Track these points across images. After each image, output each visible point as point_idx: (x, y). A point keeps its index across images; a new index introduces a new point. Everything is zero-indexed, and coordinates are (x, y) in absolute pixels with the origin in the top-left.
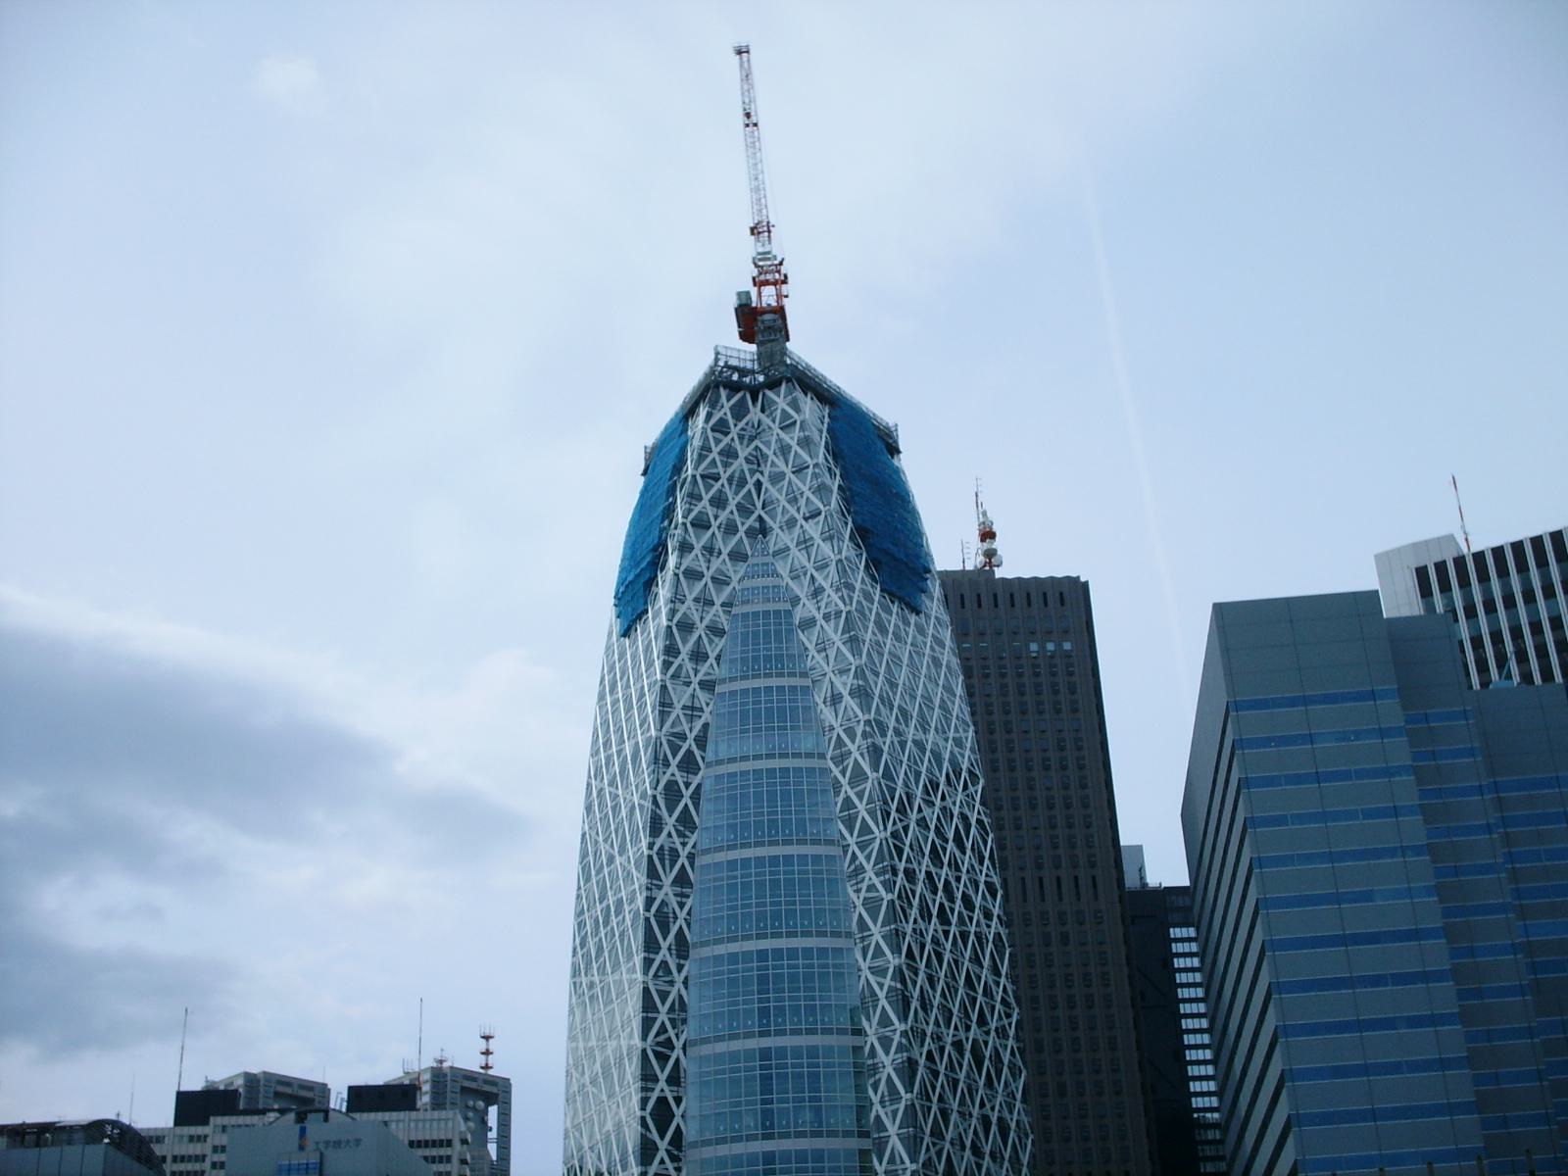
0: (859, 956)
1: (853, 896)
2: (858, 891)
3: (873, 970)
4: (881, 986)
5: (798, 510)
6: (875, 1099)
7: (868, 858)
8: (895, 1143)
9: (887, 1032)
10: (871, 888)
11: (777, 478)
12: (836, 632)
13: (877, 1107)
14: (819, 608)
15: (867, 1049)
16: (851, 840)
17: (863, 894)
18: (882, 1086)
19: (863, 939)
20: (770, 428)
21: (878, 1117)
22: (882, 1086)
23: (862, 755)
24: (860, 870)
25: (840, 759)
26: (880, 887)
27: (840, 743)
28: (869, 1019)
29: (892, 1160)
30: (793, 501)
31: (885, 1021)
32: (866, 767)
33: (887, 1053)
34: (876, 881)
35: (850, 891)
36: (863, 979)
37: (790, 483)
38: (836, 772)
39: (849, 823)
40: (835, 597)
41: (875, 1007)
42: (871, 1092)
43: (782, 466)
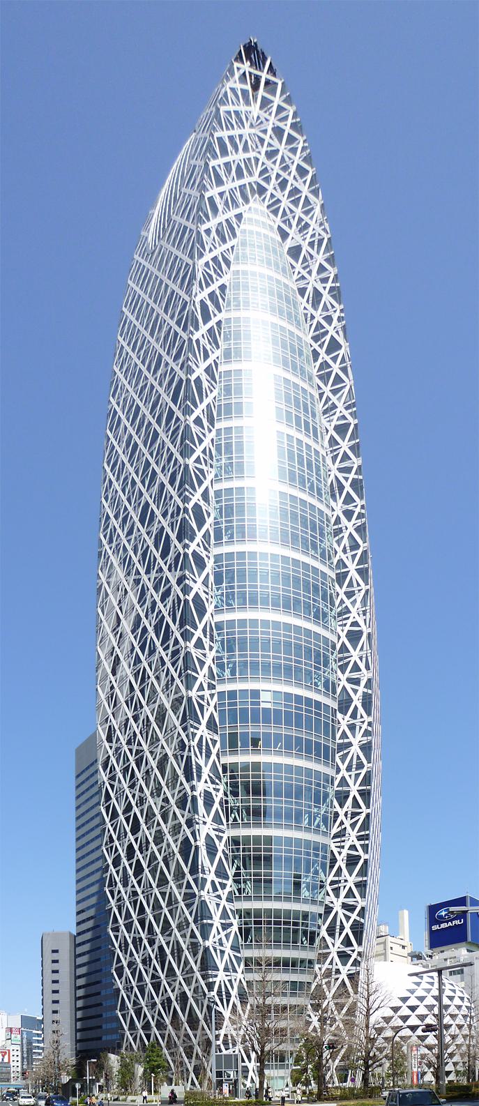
0: (329, 461)
1: (327, 425)
3: (340, 470)
4: (347, 479)
7: (339, 399)
8: (353, 574)
9: (350, 507)
12: (318, 252)
13: (340, 554)
17: (333, 424)
20: (267, 120)
21: (341, 561)
22: (345, 541)
23: (337, 332)
26: (348, 416)
28: (335, 500)
29: (350, 584)
30: (285, 168)
32: (341, 340)
33: (349, 520)
34: (346, 413)
37: (283, 157)
38: (316, 346)
42: (335, 545)
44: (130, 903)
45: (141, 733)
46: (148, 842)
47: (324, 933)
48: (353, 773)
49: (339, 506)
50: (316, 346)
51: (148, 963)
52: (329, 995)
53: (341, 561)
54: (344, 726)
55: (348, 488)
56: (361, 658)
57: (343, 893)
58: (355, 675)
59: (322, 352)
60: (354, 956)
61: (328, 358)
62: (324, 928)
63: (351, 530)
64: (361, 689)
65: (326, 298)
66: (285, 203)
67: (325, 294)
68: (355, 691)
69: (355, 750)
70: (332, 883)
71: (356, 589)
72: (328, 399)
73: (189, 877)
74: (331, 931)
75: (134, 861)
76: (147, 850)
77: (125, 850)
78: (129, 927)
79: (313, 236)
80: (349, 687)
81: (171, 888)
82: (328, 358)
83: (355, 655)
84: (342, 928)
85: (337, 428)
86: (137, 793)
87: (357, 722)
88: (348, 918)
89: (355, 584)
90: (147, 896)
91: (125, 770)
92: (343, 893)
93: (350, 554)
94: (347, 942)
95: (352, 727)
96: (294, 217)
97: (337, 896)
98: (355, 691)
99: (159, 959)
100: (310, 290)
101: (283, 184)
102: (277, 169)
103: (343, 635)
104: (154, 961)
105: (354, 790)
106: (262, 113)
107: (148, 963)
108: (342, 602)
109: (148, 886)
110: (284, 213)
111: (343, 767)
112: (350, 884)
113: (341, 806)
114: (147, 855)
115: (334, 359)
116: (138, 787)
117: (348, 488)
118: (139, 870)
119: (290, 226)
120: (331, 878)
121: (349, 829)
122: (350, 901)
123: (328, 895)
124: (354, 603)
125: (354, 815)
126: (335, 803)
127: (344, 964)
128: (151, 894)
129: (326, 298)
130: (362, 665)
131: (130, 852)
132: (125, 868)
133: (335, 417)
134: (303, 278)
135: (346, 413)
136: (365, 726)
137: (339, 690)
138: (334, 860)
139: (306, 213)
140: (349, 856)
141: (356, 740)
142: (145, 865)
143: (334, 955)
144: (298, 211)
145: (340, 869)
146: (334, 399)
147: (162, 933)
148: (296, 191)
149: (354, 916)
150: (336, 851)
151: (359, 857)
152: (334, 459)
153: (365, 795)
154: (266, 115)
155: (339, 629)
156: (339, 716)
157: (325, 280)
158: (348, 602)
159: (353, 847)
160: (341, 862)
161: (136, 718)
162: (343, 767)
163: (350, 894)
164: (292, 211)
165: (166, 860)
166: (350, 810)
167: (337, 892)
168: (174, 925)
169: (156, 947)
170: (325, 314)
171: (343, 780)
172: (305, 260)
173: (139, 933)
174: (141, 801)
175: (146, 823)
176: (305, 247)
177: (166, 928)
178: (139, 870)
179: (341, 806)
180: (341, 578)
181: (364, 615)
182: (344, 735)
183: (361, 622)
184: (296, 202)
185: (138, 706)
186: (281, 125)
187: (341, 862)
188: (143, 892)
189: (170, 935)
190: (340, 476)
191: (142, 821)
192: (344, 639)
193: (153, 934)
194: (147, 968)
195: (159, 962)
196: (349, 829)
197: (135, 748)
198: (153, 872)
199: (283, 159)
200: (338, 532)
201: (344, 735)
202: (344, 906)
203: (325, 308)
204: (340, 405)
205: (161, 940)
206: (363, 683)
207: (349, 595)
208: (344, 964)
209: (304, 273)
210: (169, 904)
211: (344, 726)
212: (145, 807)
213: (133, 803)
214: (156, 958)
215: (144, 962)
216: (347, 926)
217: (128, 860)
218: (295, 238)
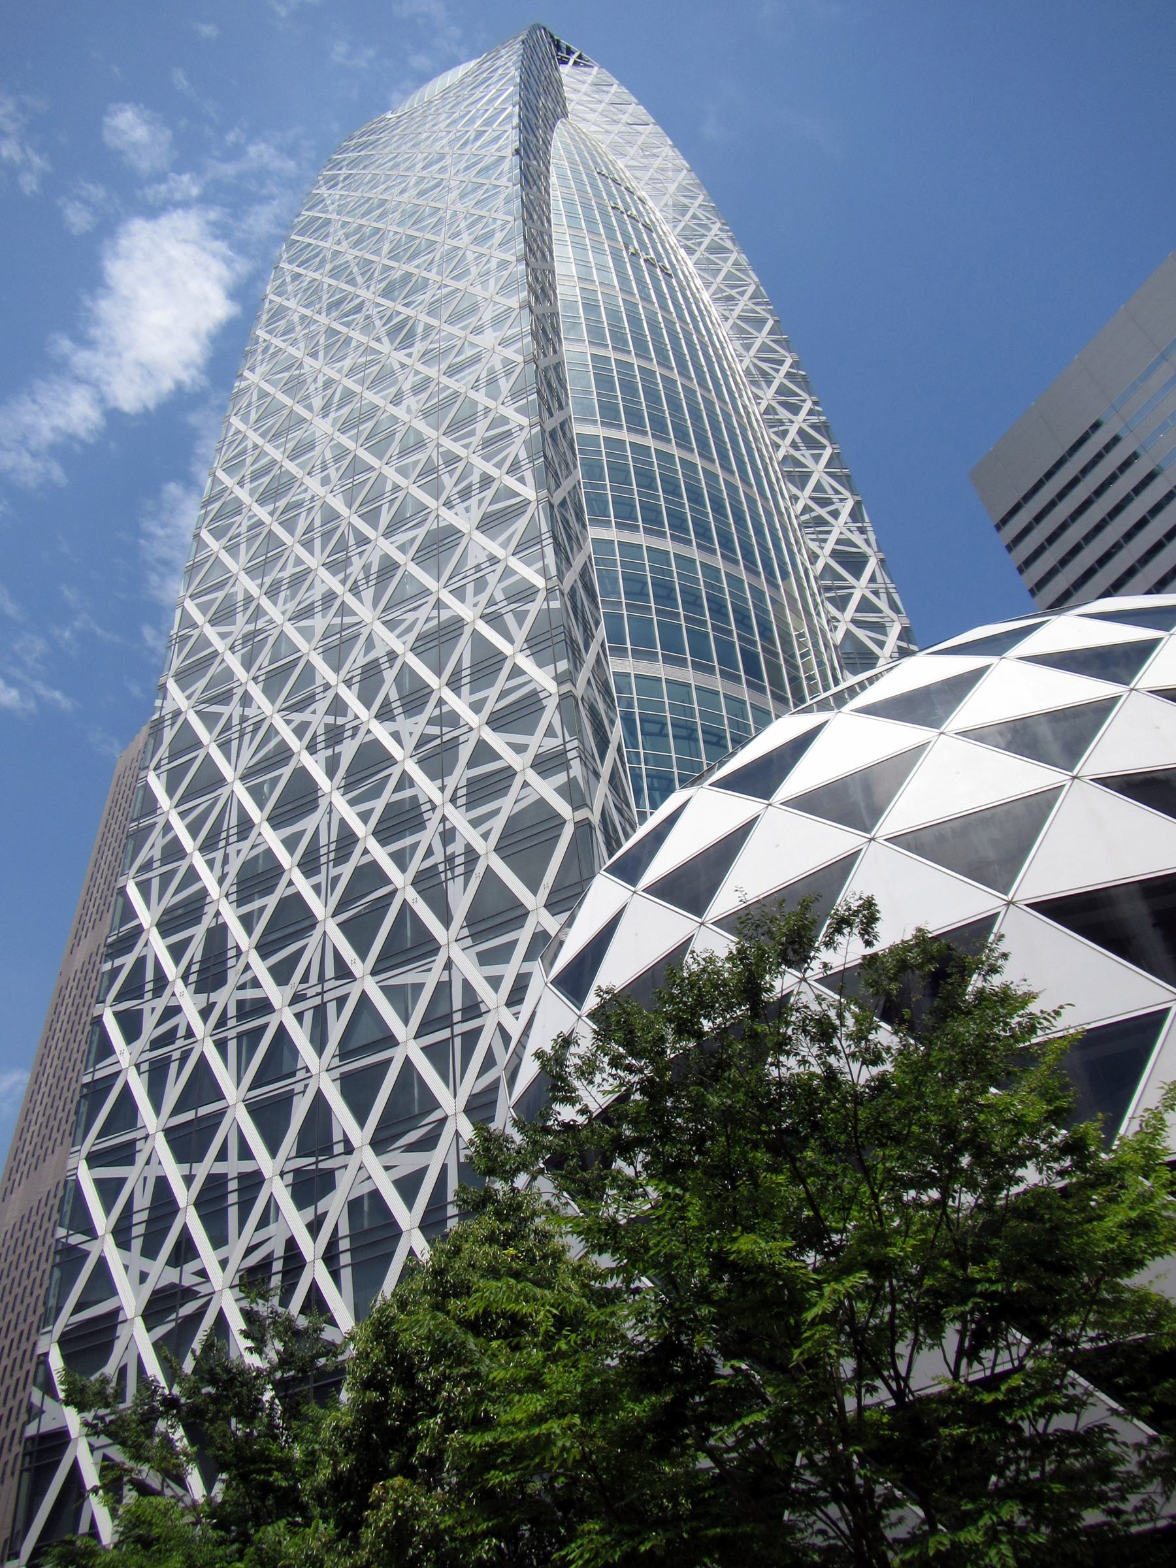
44: (221, 1045)
51: (276, 1280)
56: (876, 593)
58: (871, 617)
76: (342, 857)
77: (231, 878)
81: (449, 965)
89: (830, 491)
90: (320, 1012)
93: (808, 453)
98: (881, 644)
99: (345, 1259)
107: (276, 1280)
109: (330, 972)
114: (336, 879)
116: (322, 706)
124: (835, 514)
128: (341, 1001)
131: (257, 878)
132: (219, 933)
147: (379, 1144)
169: (335, 1205)
173: (246, 1153)
175: (347, 788)
181: (862, 531)
185: (352, 541)
188: (297, 998)
193: (326, 1149)
195: (346, 1275)
205: (367, 1169)
212: (348, 750)
214: (330, 1257)
215: (253, 1280)
217: (240, 903)
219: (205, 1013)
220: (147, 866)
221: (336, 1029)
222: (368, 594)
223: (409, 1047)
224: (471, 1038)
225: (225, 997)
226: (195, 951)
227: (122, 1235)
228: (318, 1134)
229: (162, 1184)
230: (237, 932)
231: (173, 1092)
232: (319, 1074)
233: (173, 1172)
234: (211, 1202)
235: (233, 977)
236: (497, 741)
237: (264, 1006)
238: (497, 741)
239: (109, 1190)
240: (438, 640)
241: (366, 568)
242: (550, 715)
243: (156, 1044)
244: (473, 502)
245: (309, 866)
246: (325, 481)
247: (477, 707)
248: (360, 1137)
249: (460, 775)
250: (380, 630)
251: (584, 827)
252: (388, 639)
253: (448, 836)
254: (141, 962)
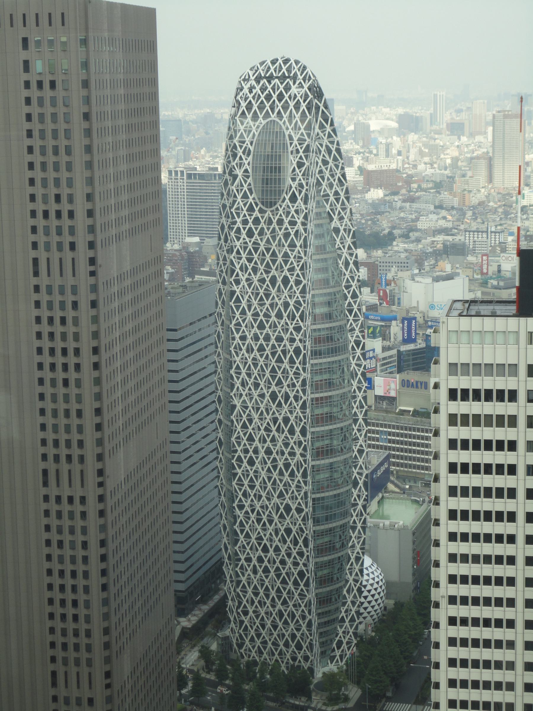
0: (351, 359)
1: (350, 338)
2: (352, 337)
3: (356, 365)
4: (359, 370)
5: (334, 180)
6: (355, 406)
7: (357, 326)
8: (361, 420)
10: (358, 336)
11: (325, 163)
13: (355, 409)
14: (341, 225)
15: (353, 390)
16: (351, 318)
17: (354, 338)
18: (358, 403)
19: (353, 353)
21: (355, 412)
22: (358, 403)
24: (353, 330)
25: (348, 287)
27: (348, 281)
29: (360, 426)
31: (360, 382)
34: (360, 335)
35: (349, 336)
36: (352, 368)
38: (346, 291)
39: (350, 312)
40: (349, 223)
41: (356, 377)
43: (328, 158)
45: (272, 508)
46: (275, 562)
47: (345, 592)
48: (359, 518)
49: (355, 384)
50: (346, 291)
52: (347, 621)
53: (355, 412)
54: (355, 495)
55: (359, 376)
57: (354, 574)
58: (360, 471)
59: (349, 296)
60: (358, 603)
61: (351, 301)
62: (345, 590)
63: (360, 398)
64: (363, 478)
65: (352, 265)
66: (332, 198)
67: (351, 262)
68: (360, 479)
69: (360, 507)
70: (349, 569)
71: (362, 428)
72: (351, 324)
73: (302, 586)
74: (348, 591)
75: (264, 565)
78: (256, 594)
79: (346, 225)
80: (357, 476)
82: (351, 301)
83: (361, 461)
84: (353, 590)
85: (355, 341)
86: (268, 535)
87: (361, 494)
88: (355, 586)
91: (259, 521)
92: (354, 574)
93: (360, 410)
94: (355, 597)
95: (359, 496)
96: (336, 209)
97: (351, 575)
98: (360, 479)
100: (343, 257)
101: (331, 186)
102: (327, 174)
103: (356, 450)
104: (274, 615)
105: (359, 525)
106: (320, 132)
108: (356, 434)
110: (331, 205)
111: (354, 515)
112: (357, 570)
113: (354, 533)
115: (355, 302)
117: (359, 376)
118: (266, 571)
119: (335, 215)
120: (348, 567)
121: (356, 544)
122: (356, 578)
123: (346, 574)
124: (361, 435)
125: (359, 538)
126: (351, 531)
127: (353, 606)
129: (352, 265)
130: (364, 467)
131: (260, 560)
132: (255, 566)
133: (355, 335)
134: (340, 249)
135: (360, 335)
136: (364, 496)
137: (353, 477)
138: (350, 558)
139: (344, 209)
140: (356, 557)
141: (360, 503)
142: (272, 571)
143: (349, 602)
144: (339, 206)
145: (352, 563)
146: (354, 325)
148: (336, 193)
149: (358, 585)
150: (350, 554)
151: (360, 558)
152: (354, 358)
153: (364, 528)
154: (321, 135)
155: (354, 447)
156: (353, 490)
157: (351, 255)
158: (358, 435)
159: (358, 553)
160: (353, 560)
161: (269, 499)
162: (354, 515)
163: (357, 575)
164: (335, 205)
165: (287, 574)
166: (358, 535)
167: (351, 574)
168: (291, 604)
169: (277, 609)
170: (351, 275)
171: (354, 522)
172: (341, 239)
174: (271, 540)
176: (342, 231)
177: (285, 603)
178: (266, 571)
179: (354, 533)
180: (356, 421)
182: (355, 500)
183: (364, 446)
184: (337, 200)
186: (330, 146)
187: (353, 560)
189: (288, 607)
190: (356, 368)
191: (271, 550)
192: (356, 452)
194: (269, 617)
196: (356, 544)
197: (267, 513)
198: (278, 576)
199: (331, 170)
200: (354, 397)
201: (355, 500)
202: (355, 580)
203: (351, 272)
204: (357, 329)
205: (279, 606)
206: (364, 475)
207: (359, 430)
208: (353, 606)
209: (341, 246)
210: (289, 593)
211: (355, 495)
213: (265, 539)
215: (267, 613)
216: (355, 589)
218: (336, 223)
219: (255, 578)
220: (239, 547)
221: (275, 589)
222: (275, 511)
223: (285, 595)
224: (293, 598)
225: (258, 576)
226: (251, 566)
227: (247, 601)
228: (273, 600)
229: (252, 598)
230: (258, 567)
231: (252, 587)
232: (273, 593)
233: (254, 598)
234: (260, 602)
235: (259, 575)
236: (297, 557)
237: (264, 581)
238: (297, 557)
239: (245, 596)
240: (288, 531)
241: (274, 504)
242: (305, 557)
243: (248, 579)
244: (294, 501)
245: (269, 561)
246: (263, 469)
247: (295, 549)
248: (280, 603)
249: (292, 559)
250: (278, 523)
251: (308, 577)
252: (279, 525)
253: (290, 568)
254: (242, 565)
